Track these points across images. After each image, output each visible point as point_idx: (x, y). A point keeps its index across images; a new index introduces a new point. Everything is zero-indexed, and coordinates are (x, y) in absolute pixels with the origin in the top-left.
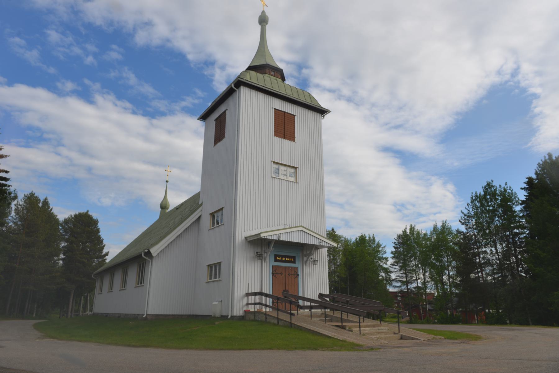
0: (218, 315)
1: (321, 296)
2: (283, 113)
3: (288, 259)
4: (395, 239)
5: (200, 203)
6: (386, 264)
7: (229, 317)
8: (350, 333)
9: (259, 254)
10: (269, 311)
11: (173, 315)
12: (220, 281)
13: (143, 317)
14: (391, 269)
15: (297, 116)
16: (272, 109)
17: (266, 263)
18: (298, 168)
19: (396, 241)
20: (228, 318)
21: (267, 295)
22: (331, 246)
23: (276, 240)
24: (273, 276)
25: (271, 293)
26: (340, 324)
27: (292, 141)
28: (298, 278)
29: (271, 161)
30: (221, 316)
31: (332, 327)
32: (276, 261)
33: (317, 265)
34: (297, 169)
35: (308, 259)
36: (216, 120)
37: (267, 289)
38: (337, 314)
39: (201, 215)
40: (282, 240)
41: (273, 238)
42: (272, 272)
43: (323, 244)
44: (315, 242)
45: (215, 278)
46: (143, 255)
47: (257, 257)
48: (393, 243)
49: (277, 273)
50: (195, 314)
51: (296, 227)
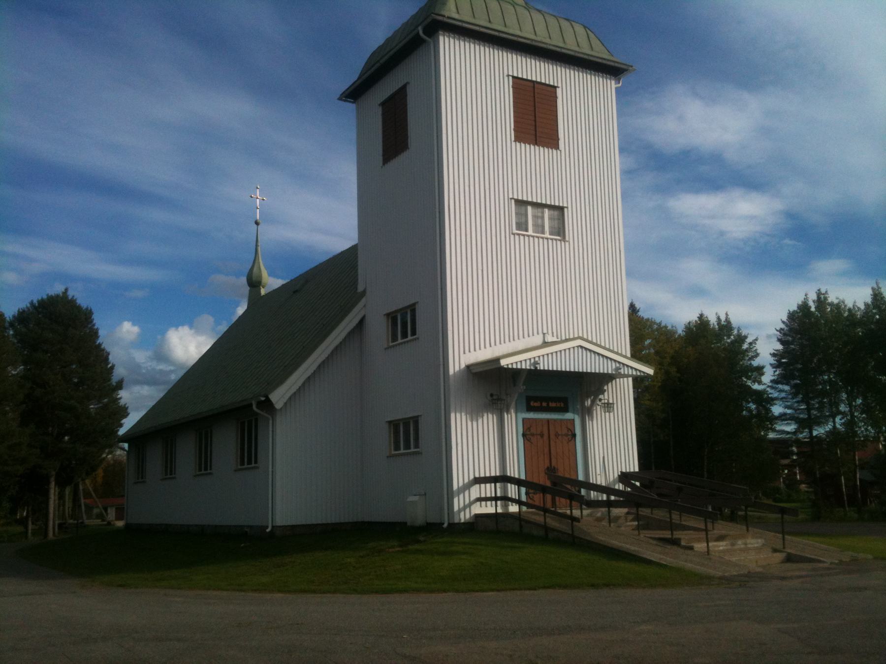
0: (420, 521)
1: (625, 477)
2: (532, 84)
3: (553, 405)
4: (783, 322)
6: (760, 383)
7: (445, 525)
8: (689, 552)
9: (495, 397)
10: (526, 512)
12: (419, 454)
14: (771, 394)
15: (562, 89)
16: (506, 79)
17: (509, 415)
18: (566, 207)
19: (783, 326)
20: (443, 527)
21: (518, 482)
22: (642, 374)
23: (529, 371)
24: (526, 441)
25: (523, 477)
26: (667, 534)
27: (552, 149)
28: (575, 440)
29: (511, 199)
30: (427, 523)
31: (651, 541)
32: (530, 409)
33: (612, 414)
34: (566, 210)
35: (593, 402)
37: (515, 469)
38: (660, 514)
40: (542, 368)
41: (524, 367)
42: (522, 432)
43: (626, 371)
44: (607, 368)
45: (407, 446)
47: (493, 404)
48: (777, 331)
49: (533, 435)
50: (367, 519)
51: (567, 340)
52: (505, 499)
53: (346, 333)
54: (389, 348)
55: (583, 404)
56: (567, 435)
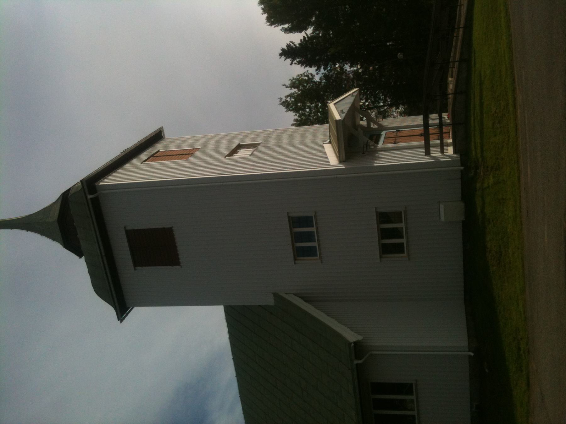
5: (270, 301)
7: (462, 168)
11: (468, 338)
13: (474, 356)
36: (136, 263)
39: (295, 295)
46: (360, 362)
52: (441, 125)
53: (306, 303)
54: (321, 258)
55: (376, 129)
56: (397, 133)
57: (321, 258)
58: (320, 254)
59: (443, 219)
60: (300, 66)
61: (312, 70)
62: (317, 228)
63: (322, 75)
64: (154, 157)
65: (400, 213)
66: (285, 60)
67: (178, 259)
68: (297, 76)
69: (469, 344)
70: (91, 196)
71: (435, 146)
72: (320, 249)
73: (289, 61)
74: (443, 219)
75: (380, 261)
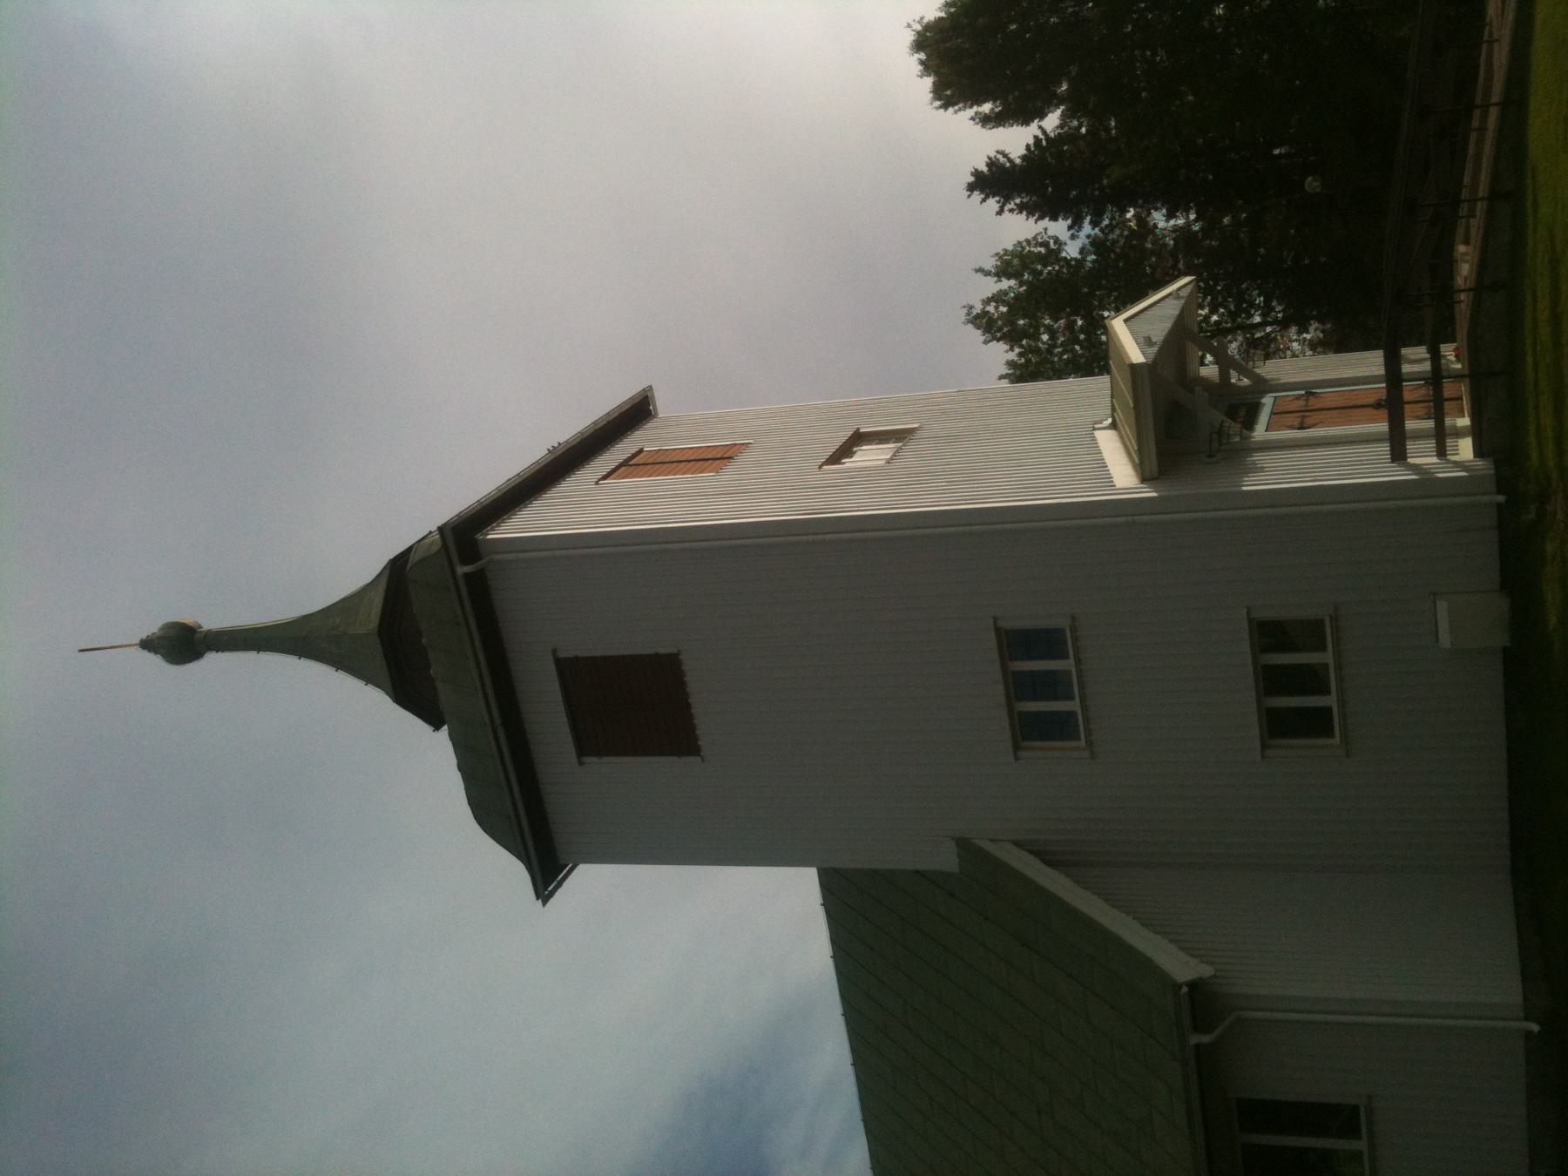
5: (947, 860)
7: (1501, 498)
13: (1539, 1032)
20: (1507, 501)
39: (1018, 844)
46: (1206, 1039)
52: (1436, 377)
53: (1049, 869)
54: (1090, 744)
56: (1307, 400)
57: (1090, 744)
58: (1089, 733)
59: (1445, 640)
60: (1025, 217)
61: (1058, 228)
62: (1078, 662)
63: (1087, 241)
64: (628, 466)
65: (1317, 625)
66: (984, 200)
67: (695, 738)
68: (1014, 245)
69: (1525, 999)
70: (467, 569)
71: (1419, 435)
72: (1087, 720)
73: (993, 203)
74: (1445, 640)
75: (1263, 756)
